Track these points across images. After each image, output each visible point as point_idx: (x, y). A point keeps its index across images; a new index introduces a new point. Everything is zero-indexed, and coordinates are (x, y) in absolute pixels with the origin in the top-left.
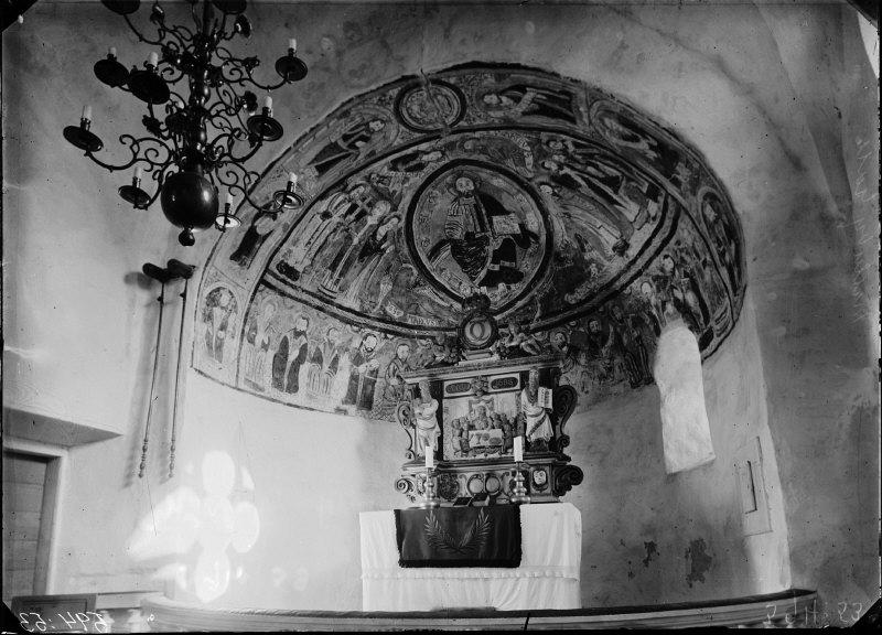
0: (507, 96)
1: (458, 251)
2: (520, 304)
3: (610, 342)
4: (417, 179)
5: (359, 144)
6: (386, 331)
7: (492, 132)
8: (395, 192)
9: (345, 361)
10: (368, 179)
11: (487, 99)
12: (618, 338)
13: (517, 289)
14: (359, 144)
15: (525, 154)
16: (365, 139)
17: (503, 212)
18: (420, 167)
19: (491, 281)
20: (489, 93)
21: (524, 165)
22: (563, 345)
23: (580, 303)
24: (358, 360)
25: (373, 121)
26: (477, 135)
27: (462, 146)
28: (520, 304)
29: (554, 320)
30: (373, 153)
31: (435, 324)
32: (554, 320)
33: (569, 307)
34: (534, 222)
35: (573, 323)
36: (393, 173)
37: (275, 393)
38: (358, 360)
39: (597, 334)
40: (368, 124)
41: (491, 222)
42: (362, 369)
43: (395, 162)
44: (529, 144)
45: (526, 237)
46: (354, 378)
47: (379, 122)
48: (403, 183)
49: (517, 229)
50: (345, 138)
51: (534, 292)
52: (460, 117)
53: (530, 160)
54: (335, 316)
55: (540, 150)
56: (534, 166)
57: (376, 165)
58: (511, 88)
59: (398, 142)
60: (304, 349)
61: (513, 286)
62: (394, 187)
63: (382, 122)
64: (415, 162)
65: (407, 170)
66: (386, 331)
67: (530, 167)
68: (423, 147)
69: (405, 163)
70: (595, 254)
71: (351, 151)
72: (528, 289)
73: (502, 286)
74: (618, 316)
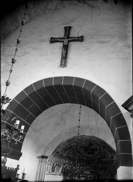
1: (84, 148)
2: (93, 158)
3: (108, 169)
6: (69, 159)
9: (62, 165)
12: (110, 170)
13: (93, 156)
17: (93, 145)
19: (89, 153)
22: (100, 167)
23: (104, 161)
24: (64, 165)
28: (93, 158)
29: (99, 162)
31: (78, 158)
32: (99, 162)
33: (102, 161)
34: (98, 148)
35: (103, 164)
37: (51, 173)
38: (64, 165)
39: (106, 167)
41: (91, 146)
42: (64, 166)
45: (96, 149)
46: (63, 168)
49: (95, 148)
51: (96, 157)
54: (62, 158)
60: (56, 164)
61: (93, 155)
66: (69, 159)
70: (107, 156)
72: (95, 156)
73: (91, 154)
74: (110, 166)
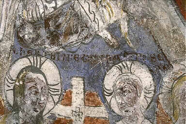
8: (113, 29)
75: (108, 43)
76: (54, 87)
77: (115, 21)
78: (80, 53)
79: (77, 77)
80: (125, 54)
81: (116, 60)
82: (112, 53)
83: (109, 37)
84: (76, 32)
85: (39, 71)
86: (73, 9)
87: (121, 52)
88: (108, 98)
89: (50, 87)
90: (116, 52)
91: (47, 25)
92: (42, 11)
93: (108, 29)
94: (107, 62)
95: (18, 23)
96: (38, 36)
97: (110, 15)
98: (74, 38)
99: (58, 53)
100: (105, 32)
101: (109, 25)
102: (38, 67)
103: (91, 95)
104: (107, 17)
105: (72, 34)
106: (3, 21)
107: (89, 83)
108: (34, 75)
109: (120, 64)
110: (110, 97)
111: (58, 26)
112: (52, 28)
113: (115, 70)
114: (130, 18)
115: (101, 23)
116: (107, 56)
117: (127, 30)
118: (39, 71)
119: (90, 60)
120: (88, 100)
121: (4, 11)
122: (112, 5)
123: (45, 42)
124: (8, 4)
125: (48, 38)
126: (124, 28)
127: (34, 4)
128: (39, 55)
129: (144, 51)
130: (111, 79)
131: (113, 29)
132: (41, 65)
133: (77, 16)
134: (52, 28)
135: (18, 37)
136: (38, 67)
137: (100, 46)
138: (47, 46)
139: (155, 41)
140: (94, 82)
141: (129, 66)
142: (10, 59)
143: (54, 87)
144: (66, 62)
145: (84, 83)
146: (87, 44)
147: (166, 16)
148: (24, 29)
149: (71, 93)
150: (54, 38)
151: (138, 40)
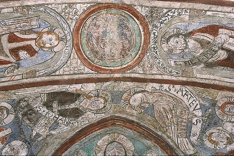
0: (196, 40)
4: (66, 129)
5: (23, 54)
7: (166, 86)
8: (38, 135)
10: (16, 104)
11: (172, 42)
14: (23, 54)
15: (194, 121)
16: (31, 51)
18: (77, 113)
20: (177, 35)
21: (188, 137)
25: (48, 33)
26: (150, 87)
27: (128, 100)
30: (33, 74)
36: (43, 110)
40: (40, 34)
43: (53, 96)
44: (202, 107)
47: (54, 37)
48: (51, 129)
50: (12, 38)
52: (139, 62)
53: (196, 129)
55: (212, 116)
56: (200, 138)
57: (29, 91)
58: (202, 31)
59: (64, 73)
62: (40, 130)
63: (59, 39)
64: (73, 106)
65: (62, 113)
67: (194, 139)
68: (91, 87)
69: (61, 103)
71: (12, 59)
75: (31, 135)
76: (3, 122)
77: (41, 135)
78: (23, 126)
79: (12, 130)
80: (29, 144)
81: (26, 141)
82: (28, 138)
83: (34, 135)
84: (30, 122)
85: (8, 114)
86: (40, 118)
87: (29, 142)
88: (7, 146)
89: (3, 121)
90: (29, 140)
91: (29, 110)
92: (35, 106)
93: (37, 133)
94: (23, 139)
95: (26, 99)
96: (24, 108)
97: (43, 132)
98: (28, 122)
99: (19, 118)
100: (35, 133)
101: (39, 133)
102: (10, 113)
103: (6, 138)
104: (41, 131)
105: (29, 120)
106: (24, 93)
107: (11, 135)
108: (5, 112)
109: (24, 144)
110: (8, 146)
111: (30, 114)
112: (29, 112)
113: (21, 142)
114: (44, 139)
115: (38, 130)
116: (25, 137)
117: (39, 140)
118: (8, 114)
119: (21, 132)
120: (3, 138)
121: (29, 92)
122: (47, 131)
123: (22, 111)
124: (33, 93)
125: (24, 112)
126: (39, 139)
127: (36, 103)
128: (15, 111)
129: (33, 149)
130: (17, 143)
131: (38, 135)
132: (10, 114)
133: (37, 120)
134: (29, 112)
135: (20, 101)
136: (10, 113)
137: (29, 133)
138: (20, 113)
139: (39, 152)
140: (12, 137)
141: (25, 147)
142: (9, 101)
143: (3, 122)
144: (17, 122)
145: (10, 133)
146: (27, 128)
147: (50, 151)
148: (24, 102)
149: (3, 130)
150: (24, 115)
151: (37, 146)
